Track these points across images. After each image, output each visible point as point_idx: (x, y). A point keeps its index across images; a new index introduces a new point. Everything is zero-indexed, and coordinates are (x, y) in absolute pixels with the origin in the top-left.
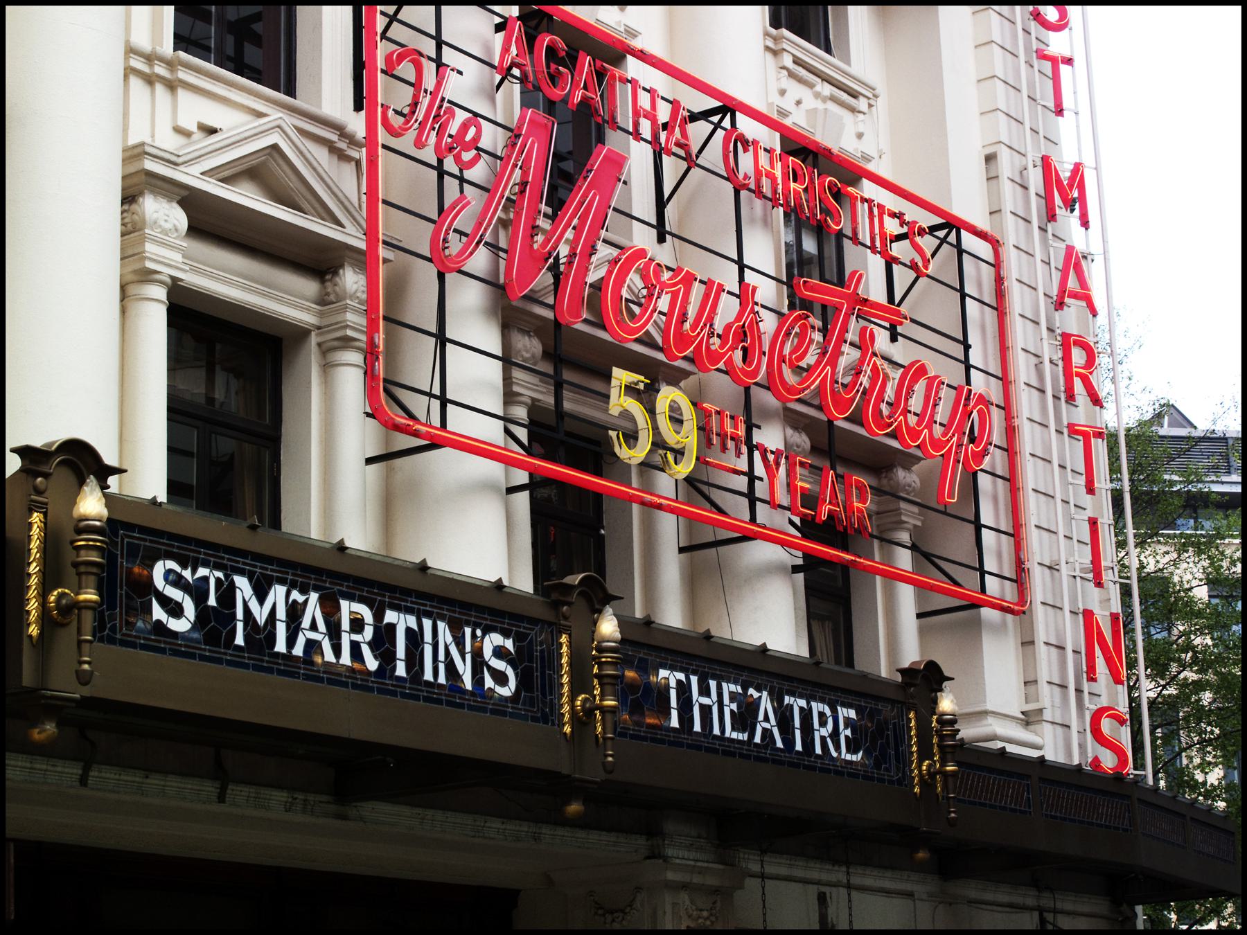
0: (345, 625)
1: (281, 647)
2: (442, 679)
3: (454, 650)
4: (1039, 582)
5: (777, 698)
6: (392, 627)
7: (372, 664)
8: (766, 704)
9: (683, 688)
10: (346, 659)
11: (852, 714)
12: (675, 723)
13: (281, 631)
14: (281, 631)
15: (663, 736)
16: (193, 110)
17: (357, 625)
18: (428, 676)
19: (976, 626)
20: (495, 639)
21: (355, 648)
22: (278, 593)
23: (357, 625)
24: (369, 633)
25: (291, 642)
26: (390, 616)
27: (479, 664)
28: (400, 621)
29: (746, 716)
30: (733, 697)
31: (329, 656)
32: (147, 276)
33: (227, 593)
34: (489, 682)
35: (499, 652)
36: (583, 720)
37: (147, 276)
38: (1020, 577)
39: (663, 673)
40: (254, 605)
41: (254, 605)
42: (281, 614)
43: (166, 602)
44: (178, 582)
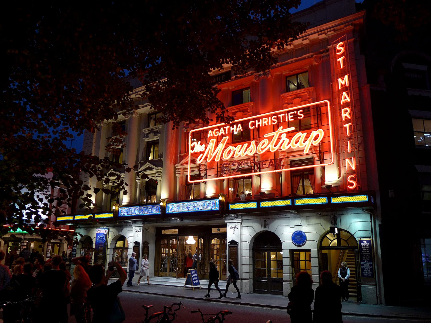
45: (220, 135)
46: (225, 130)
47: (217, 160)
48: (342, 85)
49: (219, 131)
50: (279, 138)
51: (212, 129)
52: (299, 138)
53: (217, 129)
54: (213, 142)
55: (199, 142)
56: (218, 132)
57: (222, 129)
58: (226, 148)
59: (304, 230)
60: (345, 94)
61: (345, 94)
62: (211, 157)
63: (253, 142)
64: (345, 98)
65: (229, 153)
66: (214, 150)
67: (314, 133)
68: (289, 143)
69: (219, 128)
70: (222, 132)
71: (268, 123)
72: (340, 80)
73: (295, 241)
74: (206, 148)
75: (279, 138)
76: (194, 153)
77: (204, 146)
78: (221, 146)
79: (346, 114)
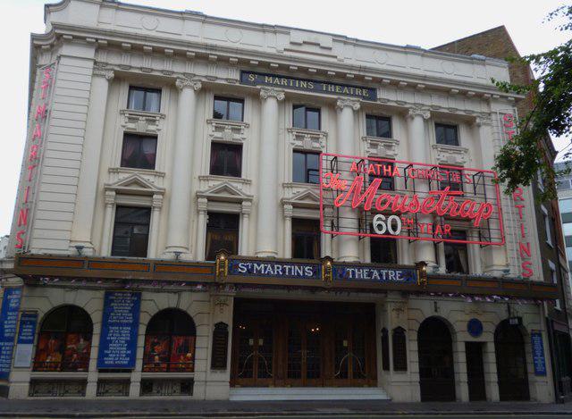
4: (508, 238)
5: (379, 271)
7: (281, 273)
8: (375, 272)
9: (353, 272)
12: (351, 276)
15: (347, 279)
16: (295, 190)
17: (278, 268)
19: (491, 249)
22: (262, 266)
23: (278, 268)
27: (304, 272)
28: (287, 267)
29: (370, 274)
32: (286, 217)
33: (253, 267)
36: (326, 278)
37: (286, 217)
38: (503, 238)
59: (481, 319)
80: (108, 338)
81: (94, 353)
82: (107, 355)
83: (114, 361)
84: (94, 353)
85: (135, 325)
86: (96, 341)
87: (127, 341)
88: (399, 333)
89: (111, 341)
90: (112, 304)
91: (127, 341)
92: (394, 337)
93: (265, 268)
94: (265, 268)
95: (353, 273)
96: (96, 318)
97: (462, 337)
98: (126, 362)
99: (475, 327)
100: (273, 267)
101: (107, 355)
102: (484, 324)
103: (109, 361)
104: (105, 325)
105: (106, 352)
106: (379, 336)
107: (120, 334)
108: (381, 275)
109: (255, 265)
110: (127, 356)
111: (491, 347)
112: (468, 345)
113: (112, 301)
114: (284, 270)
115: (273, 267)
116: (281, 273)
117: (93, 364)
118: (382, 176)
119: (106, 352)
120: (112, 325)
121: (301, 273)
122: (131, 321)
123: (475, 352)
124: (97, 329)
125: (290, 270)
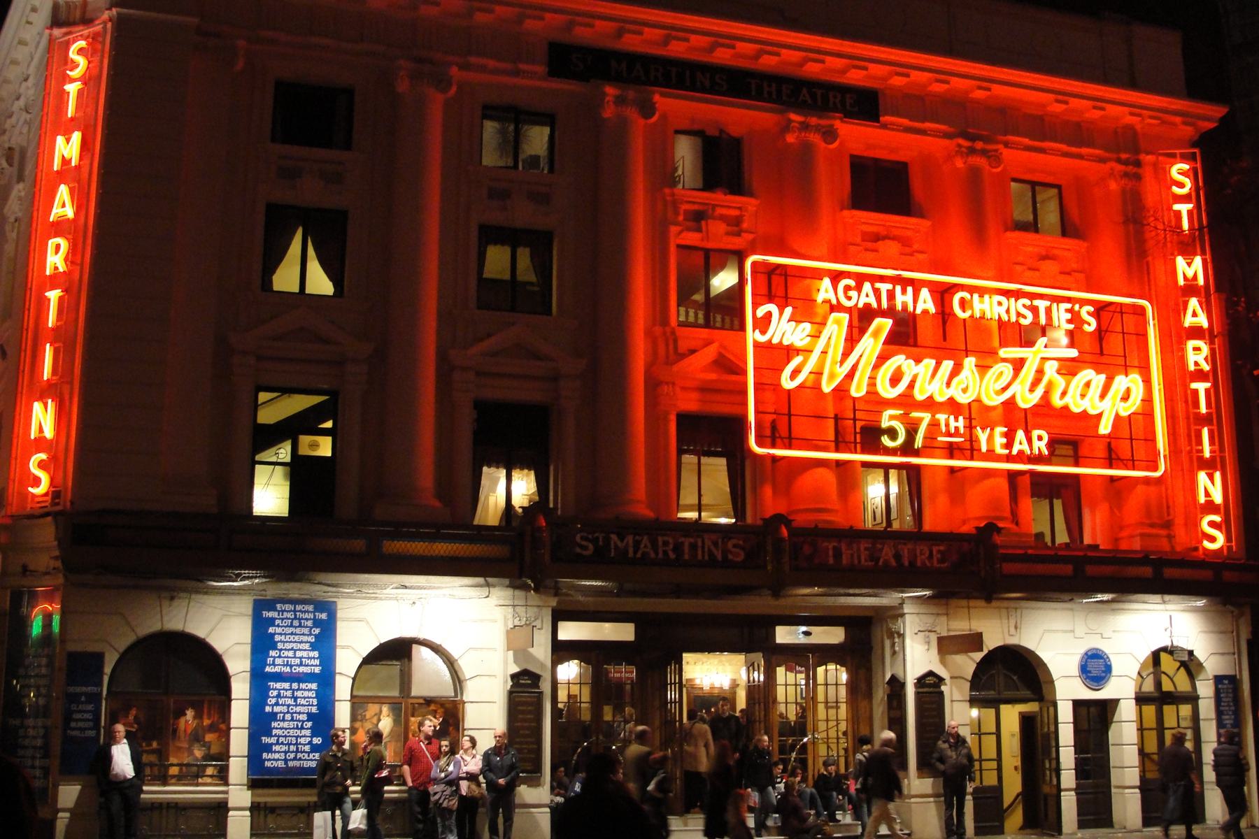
0: (660, 543)
1: (631, 554)
2: (706, 557)
3: (712, 548)
6: (682, 543)
7: (672, 556)
10: (660, 555)
11: (942, 548)
12: (831, 561)
13: (631, 551)
14: (631, 551)
17: (666, 543)
18: (700, 557)
20: (734, 541)
21: (665, 552)
22: (630, 539)
23: (666, 543)
24: (671, 546)
25: (635, 552)
26: (682, 539)
28: (687, 542)
30: (866, 549)
31: (653, 555)
33: (607, 540)
34: (730, 557)
35: (735, 546)
39: (826, 544)
40: (619, 543)
41: (619, 543)
42: (631, 542)
43: (582, 547)
44: (586, 539)
45: (860, 305)
46: (877, 293)
47: (858, 389)
48: (1185, 278)
49: (859, 288)
50: (1040, 372)
51: (836, 277)
52: (1088, 385)
53: (852, 283)
54: (838, 322)
55: (788, 311)
56: (853, 294)
57: (867, 286)
58: (882, 359)
60: (1193, 303)
61: (1193, 303)
62: (832, 376)
63: (970, 362)
64: (1196, 315)
65: (895, 380)
66: (846, 355)
67: (1121, 382)
68: (1064, 394)
69: (860, 279)
70: (866, 296)
71: (1008, 311)
72: (1180, 262)
73: (1088, 677)
74: (816, 336)
75: (1040, 372)
76: (768, 346)
77: (807, 327)
78: (870, 345)
79: (1197, 354)
80: (268, 709)
81: (239, 742)
82: (268, 748)
83: (286, 761)
84: (239, 742)
85: (326, 679)
86: (240, 713)
87: (311, 716)
88: (930, 685)
89: (273, 716)
90: (271, 630)
91: (311, 716)
92: (918, 695)
93: (637, 545)
94: (637, 545)
95: (838, 554)
96: (238, 666)
97: (1069, 688)
98: (313, 764)
99: (1095, 667)
100: (654, 544)
101: (268, 748)
102: (1111, 657)
103: (274, 760)
104: (260, 679)
105: (265, 740)
106: (880, 694)
107: (296, 699)
108: (898, 557)
109: (614, 537)
110: (314, 748)
111: (1127, 711)
112: (1078, 704)
113: (271, 622)
114: (678, 548)
115: (654, 544)
116: (672, 556)
117: (238, 768)
118: (890, 312)
119: (265, 740)
120: (279, 677)
121: (719, 557)
122: (317, 670)
123: (1094, 718)
124: (240, 689)
125: (693, 547)
